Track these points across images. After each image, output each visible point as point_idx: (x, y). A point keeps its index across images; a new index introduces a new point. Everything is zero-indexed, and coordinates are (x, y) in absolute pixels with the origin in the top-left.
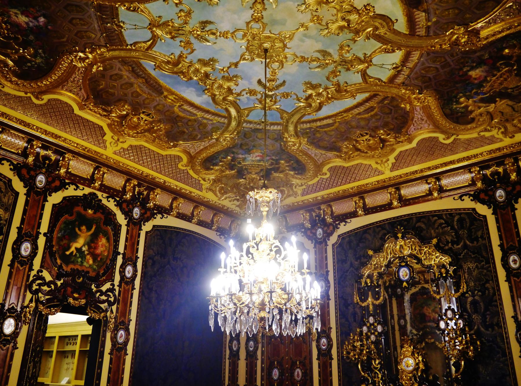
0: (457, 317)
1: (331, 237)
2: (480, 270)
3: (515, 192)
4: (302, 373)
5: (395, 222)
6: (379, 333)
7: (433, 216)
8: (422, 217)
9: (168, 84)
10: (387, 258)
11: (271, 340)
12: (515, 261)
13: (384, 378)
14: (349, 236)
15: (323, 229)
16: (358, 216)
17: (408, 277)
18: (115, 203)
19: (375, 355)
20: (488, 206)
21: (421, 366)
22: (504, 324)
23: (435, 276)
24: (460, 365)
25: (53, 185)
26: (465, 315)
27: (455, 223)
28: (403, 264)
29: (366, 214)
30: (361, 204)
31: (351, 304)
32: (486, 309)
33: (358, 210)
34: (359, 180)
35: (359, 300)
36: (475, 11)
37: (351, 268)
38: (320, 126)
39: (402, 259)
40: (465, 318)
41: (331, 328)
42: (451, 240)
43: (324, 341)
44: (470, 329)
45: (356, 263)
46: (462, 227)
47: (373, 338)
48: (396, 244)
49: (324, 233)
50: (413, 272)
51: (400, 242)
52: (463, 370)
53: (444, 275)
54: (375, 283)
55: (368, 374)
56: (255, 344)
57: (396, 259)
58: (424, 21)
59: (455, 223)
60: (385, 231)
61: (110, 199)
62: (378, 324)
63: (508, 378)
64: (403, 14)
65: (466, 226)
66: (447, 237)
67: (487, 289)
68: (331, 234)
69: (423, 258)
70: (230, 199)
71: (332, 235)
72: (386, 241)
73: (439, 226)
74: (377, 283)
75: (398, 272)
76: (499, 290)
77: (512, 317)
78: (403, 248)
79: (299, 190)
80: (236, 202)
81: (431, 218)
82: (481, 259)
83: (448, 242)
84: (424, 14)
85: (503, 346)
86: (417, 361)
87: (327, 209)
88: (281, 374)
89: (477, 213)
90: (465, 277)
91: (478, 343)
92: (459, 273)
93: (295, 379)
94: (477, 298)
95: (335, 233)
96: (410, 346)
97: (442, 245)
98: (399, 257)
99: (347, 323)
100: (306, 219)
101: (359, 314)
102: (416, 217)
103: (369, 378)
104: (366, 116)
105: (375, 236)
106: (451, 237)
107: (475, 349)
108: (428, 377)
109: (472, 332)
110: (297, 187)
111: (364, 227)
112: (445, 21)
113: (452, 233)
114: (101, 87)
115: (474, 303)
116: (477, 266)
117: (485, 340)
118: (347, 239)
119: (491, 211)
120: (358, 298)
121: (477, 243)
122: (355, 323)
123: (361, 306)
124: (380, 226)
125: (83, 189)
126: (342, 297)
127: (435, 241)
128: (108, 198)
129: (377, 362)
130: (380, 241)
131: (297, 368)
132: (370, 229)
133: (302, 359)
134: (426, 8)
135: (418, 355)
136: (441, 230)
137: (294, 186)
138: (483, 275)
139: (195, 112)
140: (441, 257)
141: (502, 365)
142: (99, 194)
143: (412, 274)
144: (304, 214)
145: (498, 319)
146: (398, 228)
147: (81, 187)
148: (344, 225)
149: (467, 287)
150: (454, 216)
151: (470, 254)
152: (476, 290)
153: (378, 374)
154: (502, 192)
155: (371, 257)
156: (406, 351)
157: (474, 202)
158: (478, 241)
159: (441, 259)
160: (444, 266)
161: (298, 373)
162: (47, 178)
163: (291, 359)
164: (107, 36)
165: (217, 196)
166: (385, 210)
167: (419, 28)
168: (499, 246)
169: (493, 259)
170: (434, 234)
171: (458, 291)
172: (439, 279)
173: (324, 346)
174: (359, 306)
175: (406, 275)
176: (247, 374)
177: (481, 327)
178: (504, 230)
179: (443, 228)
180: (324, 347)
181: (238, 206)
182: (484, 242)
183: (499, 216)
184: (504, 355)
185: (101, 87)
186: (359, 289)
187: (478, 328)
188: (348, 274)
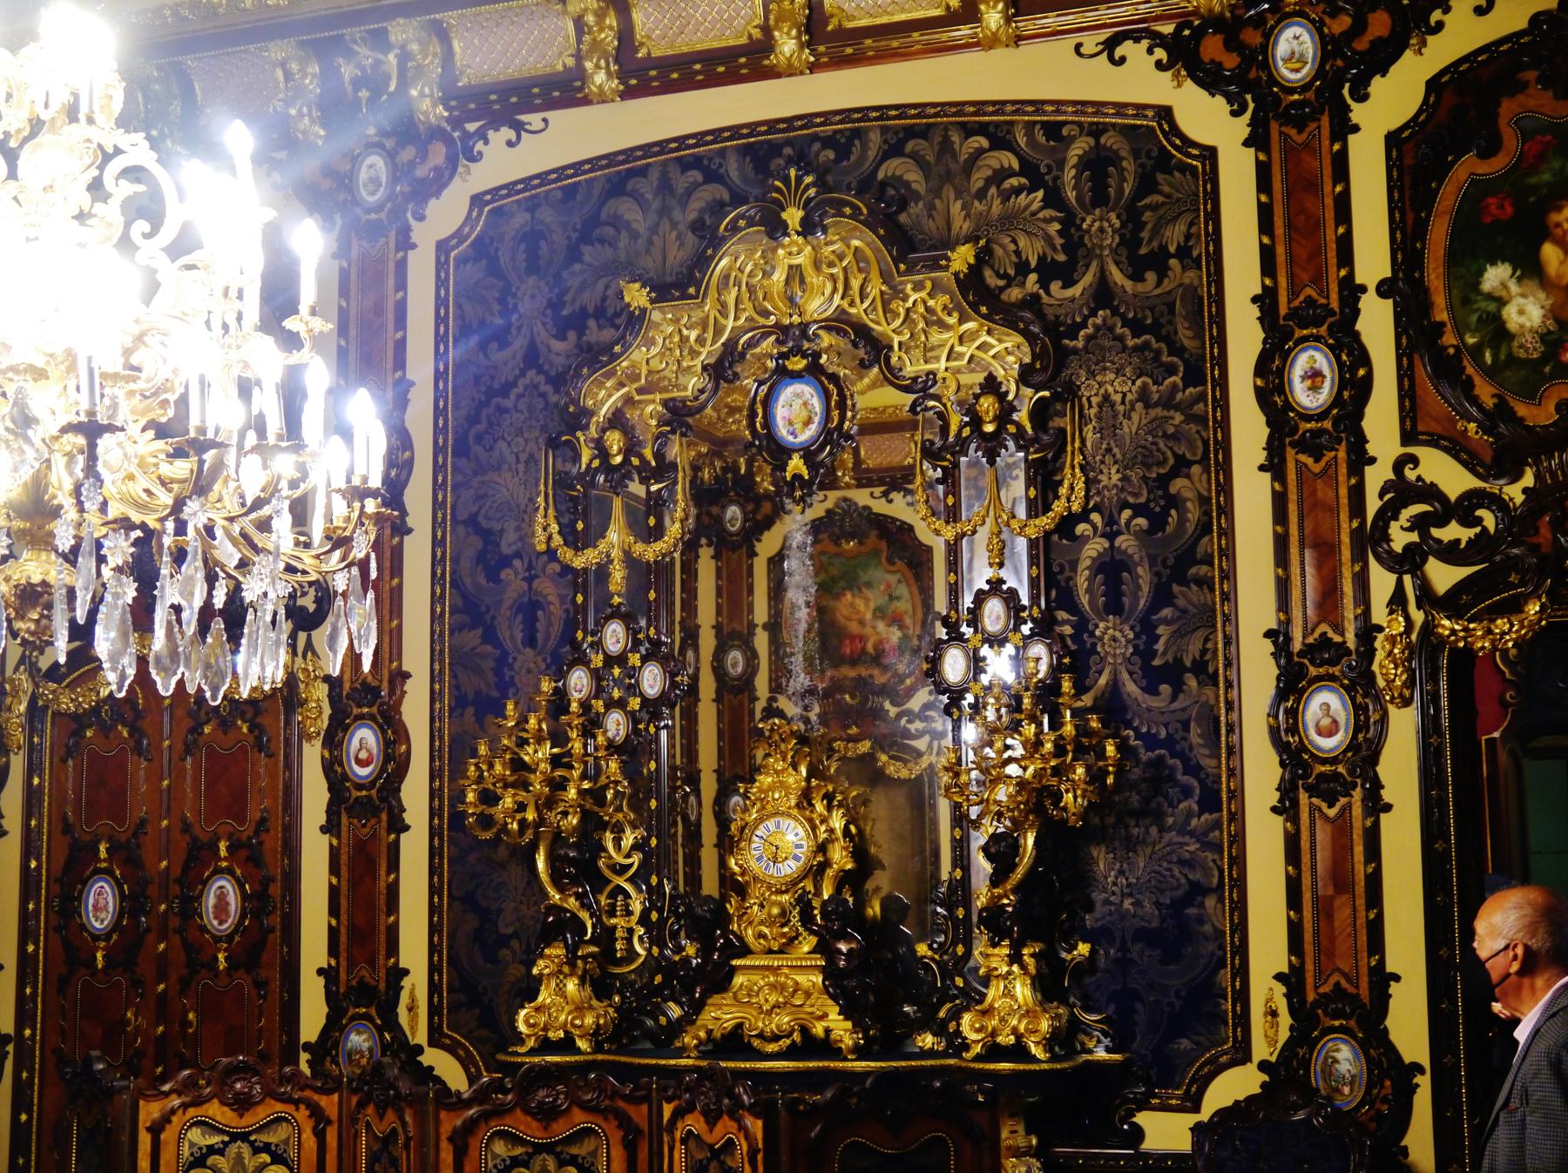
42: (1042, 259)
82: (1165, 358)
113: (1049, 221)
116: (1144, 395)
138: (1165, 436)
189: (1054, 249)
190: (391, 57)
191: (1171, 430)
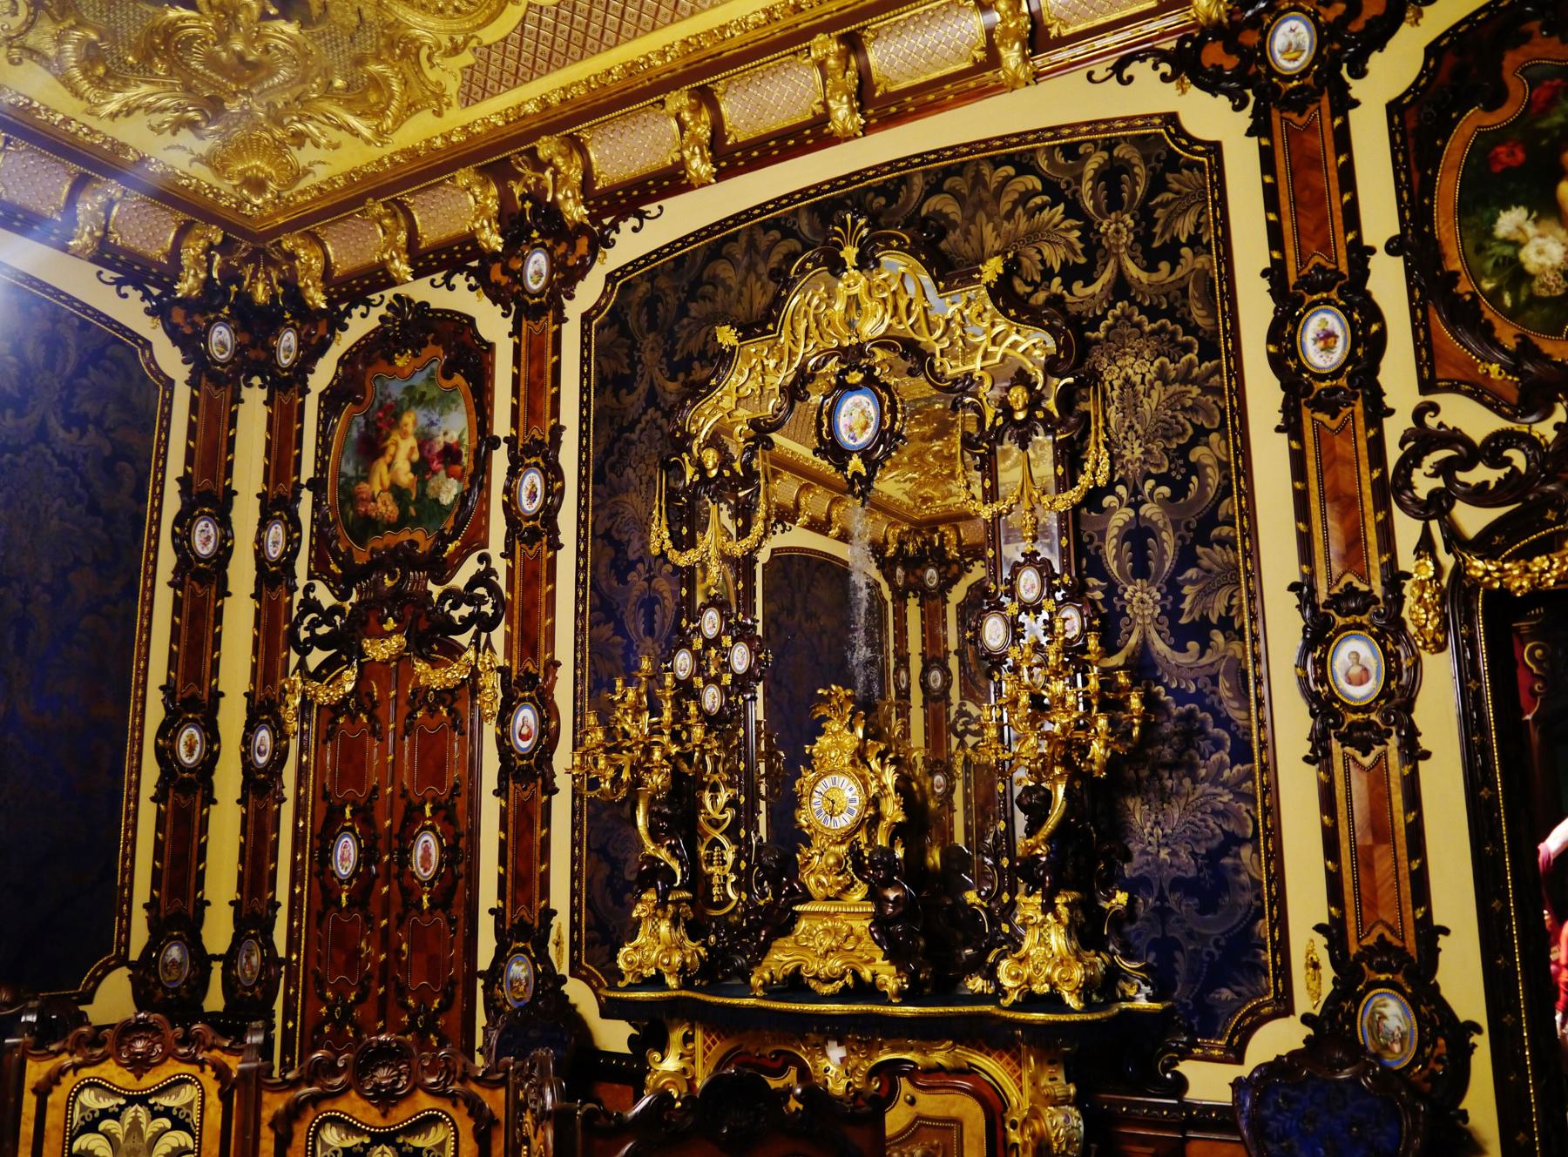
0: (1058, 595)
1: (580, 284)
2: (1176, 387)
3: (1357, 26)
4: (442, 849)
5: (838, 204)
6: (736, 677)
7: (996, 163)
8: (948, 172)
10: (791, 354)
11: (334, 721)
12: (1327, 337)
13: (743, 865)
14: (652, 276)
15: (550, 252)
16: (690, 187)
17: (870, 433)
19: (715, 771)
20: (1232, 99)
21: (892, 811)
22: (1253, 619)
23: (981, 421)
24: (1048, 798)
26: (1095, 588)
27: (1086, 187)
28: (855, 377)
29: (721, 176)
30: (704, 132)
31: (641, 560)
32: (1186, 558)
33: (687, 154)
34: (693, 13)
35: (668, 544)
37: (651, 411)
39: (852, 355)
40: (1093, 602)
41: (558, 664)
42: (1064, 264)
43: (526, 717)
44: (1109, 648)
45: (671, 386)
46: (1114, 203)
47: (712, 698)
48: (831, 295)
49: (552, 271)
50: (893, 410)
51: (853, 282)
52: (1063, 823)
53: (1020, 416)
54: (737, 466)
55: (670, 847)
56: (275, 740)
57: (833, 356)
59: (1086, 187)
60: (794, 244)
62: (734, 641)
63: (1246, 852)
65: (1133, 194)
66: (1047, 251)
67: (1195, 469)
68: (582, 271)
69: (938, 348)
70: (156, 119)
71: (582, 277)
72: (795, 281)
73: (1015, 204)
74: (746, 466)
75: (832, 413)
76: (1246, 472)
77: (1293, 587)
78: (858, 307)
79: (448, 74)
80: (185, 136)
81: (986, 170)
82: (1181, 338)
83: (1048, 274)
85: (1243, 715)
86: (874, 790)
87: (568, 156)
88: (367, 855)
89: (1181, 132)
90: (1107, 421)
91: (1135, 702)
92: (1083, 406)
93: (413, 875)
94: (1148, 510)
95: (597, 264)
96: (852, 729)
97: (1021, 288)
98: (839, 347)
99: (619, 639)
100: (483, 210)
101: (670, 604)
102: (925, 172)
103: (675, 865)
105: (751, 267)
106: (1062, 252)
107: (1118, 730)
108: (916, 854)
109: (1117, 660)
110: (436, 60)
111: (709, 230)
113: (1068, 230)
115: (1138, 536)
116: (1162, 375)
117: (1169, 691)
118: (644, 288)
119: (1244, 119)
120: (666, 534)
121: (1172, 271)
122: (649, 641)
123: (677, 569)
124: (776, 223)
126: (607, 536)
127: (992, 269)
129: (723, 796)
130: (772, 286)
131: (424, 828)
132: (734, 238)
133: (444, 794)
135: (883, 765)
136: (1023, 225)
137: (424, 52)
138: (1184, 409)
140: (1014, 337)
141: (1226, 799)
143: (888, 418)
144: (477, 190)
145: (1231, 597)
146: (843, 224)
148: (635, 230)
149: (1112, 465)
150: (1087, 156)
151: (1136, 318)
152: (1148, 476)
153: (723, 848)
154: (1302, 28)
155: (725, 358)
156: (830, 749)
157: (1173, 85)
158: (1175, 261)
159: (1014, 345)
160: (1022, 378)
161: (426, 850)
163: (404, 794)
165: (77, 94)
166: (802, 149)
168: (1264, 273)
169: (1235, 334)
170: (992, 242)
171: (1074, 483)
172: (997, 435)
173: (524, 738)
174: (669, 568)
175: (865, 428)
176: (242, 860)
177: (1154, 635)
178: (1295, 201)
179: (1031, 215)
180: (524, 744)
181: (206, 161)
182: (1202, 261)
183: (1278, 141)
184: (1242, 752)
186: (672, 496)
187: (1145, 645)
188: (634, 437)
189: (1075, 254)
190: (548, 174)
191: (1189, 403)
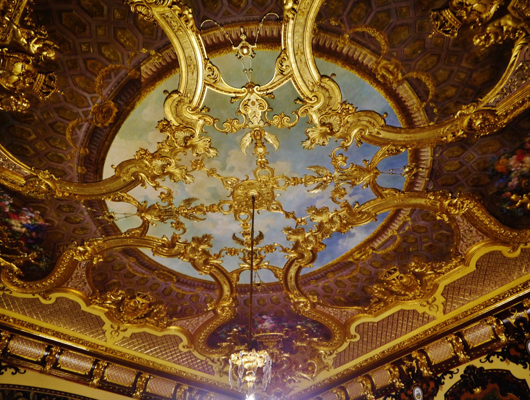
9: (333, 258)
18: (501, 357)
25: (430, 390)
36: (105, 13)
38: (420, 97)
58: (151, 61)
61: (492, 358)
64: (153, 89)
84: (142, 68)
104: (380, 39)
112: (140, 36)
114: (342, 299)
125: (458, 370)
128: (488, 359)
134: (134, 70)
139: (386, 238)
142: (476, 363)
147: (454, 370)
162: (421, 387)
164: (273, 290)
167: (165, 60)
185: (342, 299)
